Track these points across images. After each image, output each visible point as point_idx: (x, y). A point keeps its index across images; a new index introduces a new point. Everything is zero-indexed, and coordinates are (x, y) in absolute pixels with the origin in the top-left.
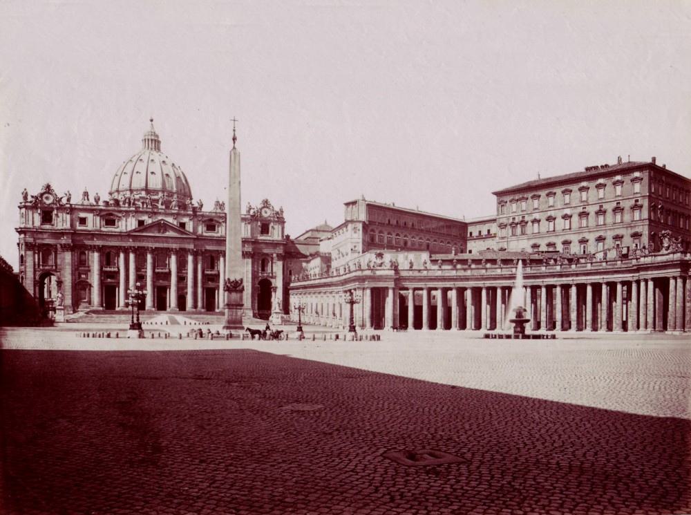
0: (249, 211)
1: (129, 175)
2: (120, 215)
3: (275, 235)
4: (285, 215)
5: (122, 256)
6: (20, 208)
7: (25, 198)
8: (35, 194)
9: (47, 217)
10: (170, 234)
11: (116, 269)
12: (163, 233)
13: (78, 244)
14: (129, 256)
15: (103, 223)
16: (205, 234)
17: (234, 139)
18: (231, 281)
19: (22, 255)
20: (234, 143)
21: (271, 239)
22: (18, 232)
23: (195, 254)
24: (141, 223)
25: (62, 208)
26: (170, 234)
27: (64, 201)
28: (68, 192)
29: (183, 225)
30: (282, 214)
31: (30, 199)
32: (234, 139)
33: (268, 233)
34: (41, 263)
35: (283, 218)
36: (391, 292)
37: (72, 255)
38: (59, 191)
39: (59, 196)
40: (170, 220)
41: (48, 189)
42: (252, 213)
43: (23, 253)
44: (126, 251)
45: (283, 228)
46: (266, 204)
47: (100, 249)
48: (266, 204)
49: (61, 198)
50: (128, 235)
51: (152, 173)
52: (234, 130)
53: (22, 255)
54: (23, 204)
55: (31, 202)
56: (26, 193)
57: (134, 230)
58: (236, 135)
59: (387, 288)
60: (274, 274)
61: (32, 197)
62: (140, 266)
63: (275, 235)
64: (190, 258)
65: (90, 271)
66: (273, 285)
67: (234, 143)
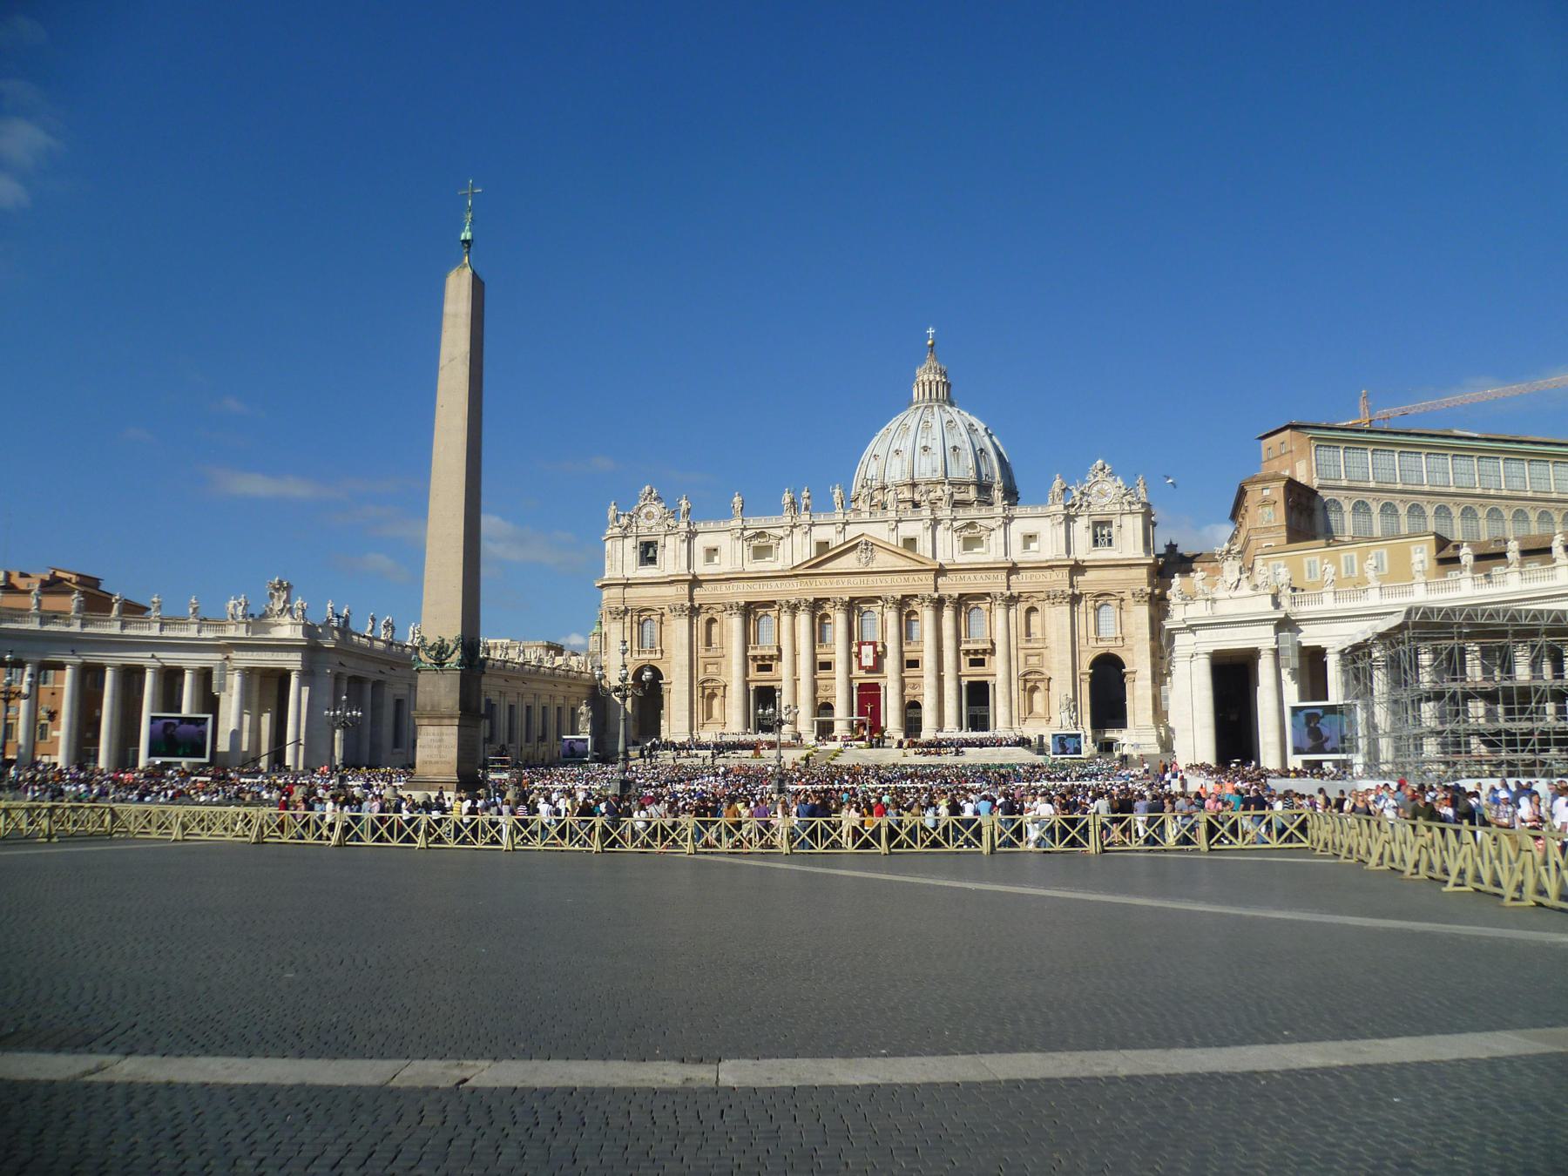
1: (881, 461)
2: (780, 532)
10: (883, 561)
11: (775, 652)
12: (867, 564)
15: (748, 553)
24: (823, 546)
29: (910, 543)
40: (879, 532)
44: (794, 609)
47: (749, 611)
51: (925, 449)
59: (1252, 656)
62: (818, 634)
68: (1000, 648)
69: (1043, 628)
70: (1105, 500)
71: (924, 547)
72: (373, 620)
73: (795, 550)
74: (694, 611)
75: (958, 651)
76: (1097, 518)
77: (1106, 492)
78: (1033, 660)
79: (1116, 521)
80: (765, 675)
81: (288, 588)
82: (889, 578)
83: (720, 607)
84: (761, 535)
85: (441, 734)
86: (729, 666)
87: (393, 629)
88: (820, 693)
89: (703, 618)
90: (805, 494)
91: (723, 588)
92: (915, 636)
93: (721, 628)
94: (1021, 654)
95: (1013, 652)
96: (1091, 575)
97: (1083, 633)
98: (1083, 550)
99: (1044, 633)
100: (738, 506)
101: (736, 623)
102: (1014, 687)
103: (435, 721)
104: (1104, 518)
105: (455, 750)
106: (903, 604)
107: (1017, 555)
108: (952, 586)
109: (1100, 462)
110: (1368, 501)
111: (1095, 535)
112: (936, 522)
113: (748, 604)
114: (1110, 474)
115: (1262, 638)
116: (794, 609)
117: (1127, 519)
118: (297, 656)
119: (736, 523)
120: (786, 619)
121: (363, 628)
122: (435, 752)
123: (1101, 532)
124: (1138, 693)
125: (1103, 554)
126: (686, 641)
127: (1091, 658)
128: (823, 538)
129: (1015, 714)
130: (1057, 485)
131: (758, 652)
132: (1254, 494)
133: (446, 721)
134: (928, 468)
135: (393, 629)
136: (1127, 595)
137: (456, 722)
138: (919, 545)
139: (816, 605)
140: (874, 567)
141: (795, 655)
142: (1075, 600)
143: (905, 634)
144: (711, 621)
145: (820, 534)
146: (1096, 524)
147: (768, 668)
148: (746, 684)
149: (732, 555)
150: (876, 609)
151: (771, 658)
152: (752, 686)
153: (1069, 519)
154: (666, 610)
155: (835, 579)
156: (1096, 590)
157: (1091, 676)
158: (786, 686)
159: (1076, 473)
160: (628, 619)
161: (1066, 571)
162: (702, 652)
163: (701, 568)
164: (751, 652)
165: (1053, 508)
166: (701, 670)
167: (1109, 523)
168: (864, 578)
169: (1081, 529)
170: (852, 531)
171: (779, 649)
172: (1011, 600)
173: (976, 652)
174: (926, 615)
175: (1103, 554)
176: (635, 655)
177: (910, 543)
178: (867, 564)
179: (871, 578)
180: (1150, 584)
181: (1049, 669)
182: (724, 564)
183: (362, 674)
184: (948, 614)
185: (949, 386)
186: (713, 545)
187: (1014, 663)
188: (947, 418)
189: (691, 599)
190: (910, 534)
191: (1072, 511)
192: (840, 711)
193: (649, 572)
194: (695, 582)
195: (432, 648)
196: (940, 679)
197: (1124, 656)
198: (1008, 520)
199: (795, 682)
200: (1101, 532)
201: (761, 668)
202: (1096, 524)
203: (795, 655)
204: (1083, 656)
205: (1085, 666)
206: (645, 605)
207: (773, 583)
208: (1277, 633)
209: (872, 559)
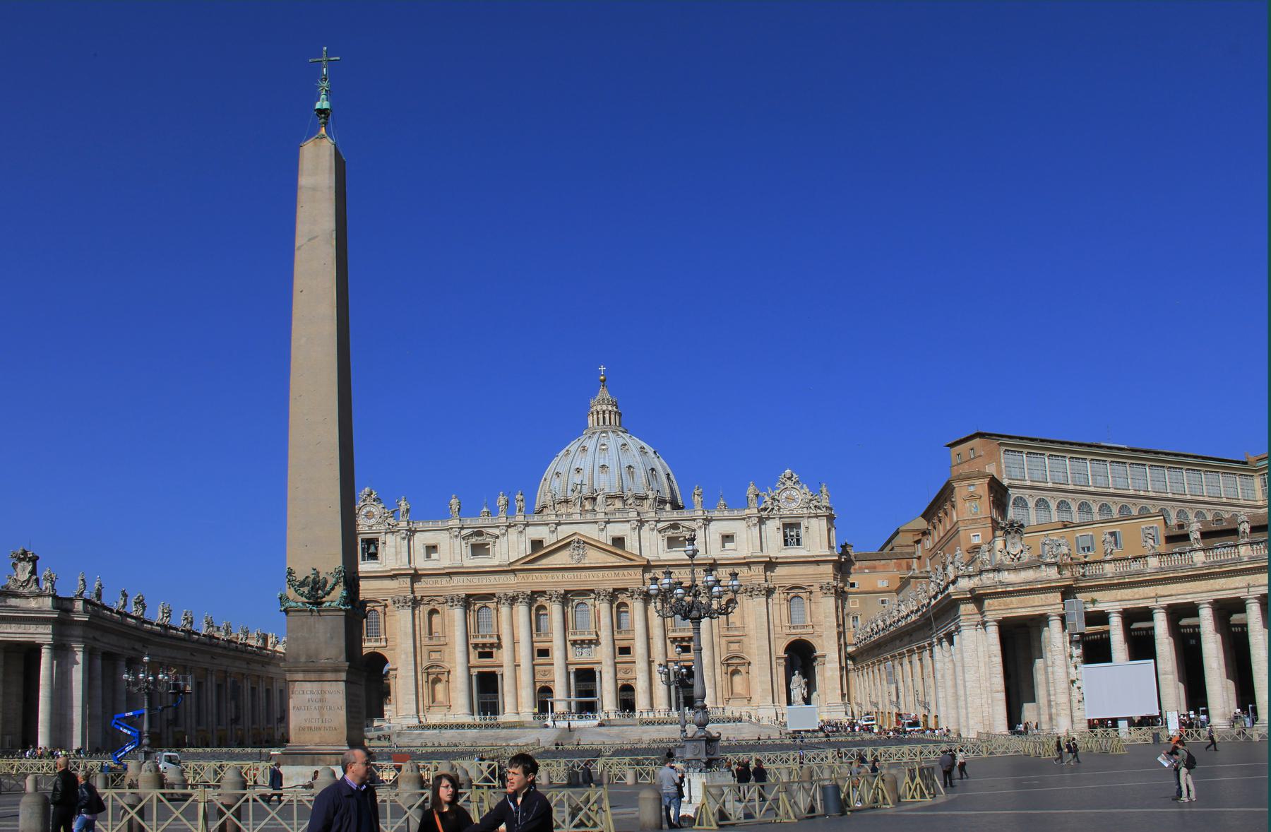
5: (504, 610)
10: (594, 558)
11: (495, 640)
12: (579, 560)
23: (647, 597)
29: (619, 542)
36: (1055, 625)
40: (590, 532)
44: (513, 600)
47: (468, 602)
59: (1040, 621)
62: (536, 626)
66: (818, 653)
69: (743, 617)
70: (794, 505)
71: (631, 545)
72: (125, 595)
73: (510, 547)
74: (416, 603)
76: (788, 521)
77: (794, 497)
78: (734, 647)
79: (804, 523)
80: (487, 661)
81: (34, 560)
82: (601, 573)
83: (442, 599)
85: (323, 692)
86: (452, 653)
87: (144, 608)
88: (538, 677)
89: (424, 610)
90: (519, 497)
91: (444, 582)
92: (624, 627)
93: (443, 619)
94: (723, 641)
95: (716, 639)
96: (779, 571)
97: (777, 622)
98: (774, 546)
99: (743, 622)
100: (455, 507)
101: (458, 612)
102: (718, 671)
103: (313, 676)
104: (793, 521)
105: (343, 712)
106: (613, 595)
109: (788, 471)
110: (1048, 499)
111: (785, 536)
112: (641, 523)
113: (468, 596)
114: (797, 482)
115: (1050, 604)
116: (513, 600)
117: (814, 521)
118: (48, 629)
119: (455, 522)
120: (504, 610)
121: (113, 601)
122: (316, 715)
123: (791, 533)
124: (828, 674)
125: (793, 552)
126: (411, 630)
127: (785, 644)
128: (537, 537)
129: (719, 694)
130: (751, 490)
131: (480, 640)
132: (961, 490)
133: (329, 676)
134: (607, 483)
135: (144, 608)
136: (816, 589)
137: (343, 676)
138: (627, 543)
139: (533, 597)
140: (586, 562)
141: (514, 642)
142: (769, 592)
143: (617, 626)
144: (433, 612)
146: (786, 526)
147: (490, 655)
149: (453, 552)
150: (589, 601)
151: (492, 645)
152: (474, 672)
153: (762, 521)
154: (390, 602)
155: (550, 574)
156: (788, 583)
157: (786, 659)
158: (507, 672)
159: (768, 480)
161: (762, 567)
162: (426, 641)
164: (472, 641)
165: (747, 511)
166: (425, 656)
167: (798, 525)
168: (577, 573)
169: (773, 527)
171: (499, 638)
174: (637, 606)
175: (793, 552)
177: (619, 542)
178: (579, 560)
179: (584, 573)
180: (835, 579)
181: (748, 654)
182: (442, 560)
183: (115, 650)
185: (620, 415)
187: (717, 649)
189: (413, 592)
190: (618, 534)
191: (764, 514)
192: (559, 691)
194: (416, 576)
195: (302, 584)
198: (708, 521)
200: (791, 533)
201: (482, 655)
203: (514, 642)
204: (779, 642)
205: (781, 653)
207: (492, 577)
208: (1063, 600)
209: (584, 556)
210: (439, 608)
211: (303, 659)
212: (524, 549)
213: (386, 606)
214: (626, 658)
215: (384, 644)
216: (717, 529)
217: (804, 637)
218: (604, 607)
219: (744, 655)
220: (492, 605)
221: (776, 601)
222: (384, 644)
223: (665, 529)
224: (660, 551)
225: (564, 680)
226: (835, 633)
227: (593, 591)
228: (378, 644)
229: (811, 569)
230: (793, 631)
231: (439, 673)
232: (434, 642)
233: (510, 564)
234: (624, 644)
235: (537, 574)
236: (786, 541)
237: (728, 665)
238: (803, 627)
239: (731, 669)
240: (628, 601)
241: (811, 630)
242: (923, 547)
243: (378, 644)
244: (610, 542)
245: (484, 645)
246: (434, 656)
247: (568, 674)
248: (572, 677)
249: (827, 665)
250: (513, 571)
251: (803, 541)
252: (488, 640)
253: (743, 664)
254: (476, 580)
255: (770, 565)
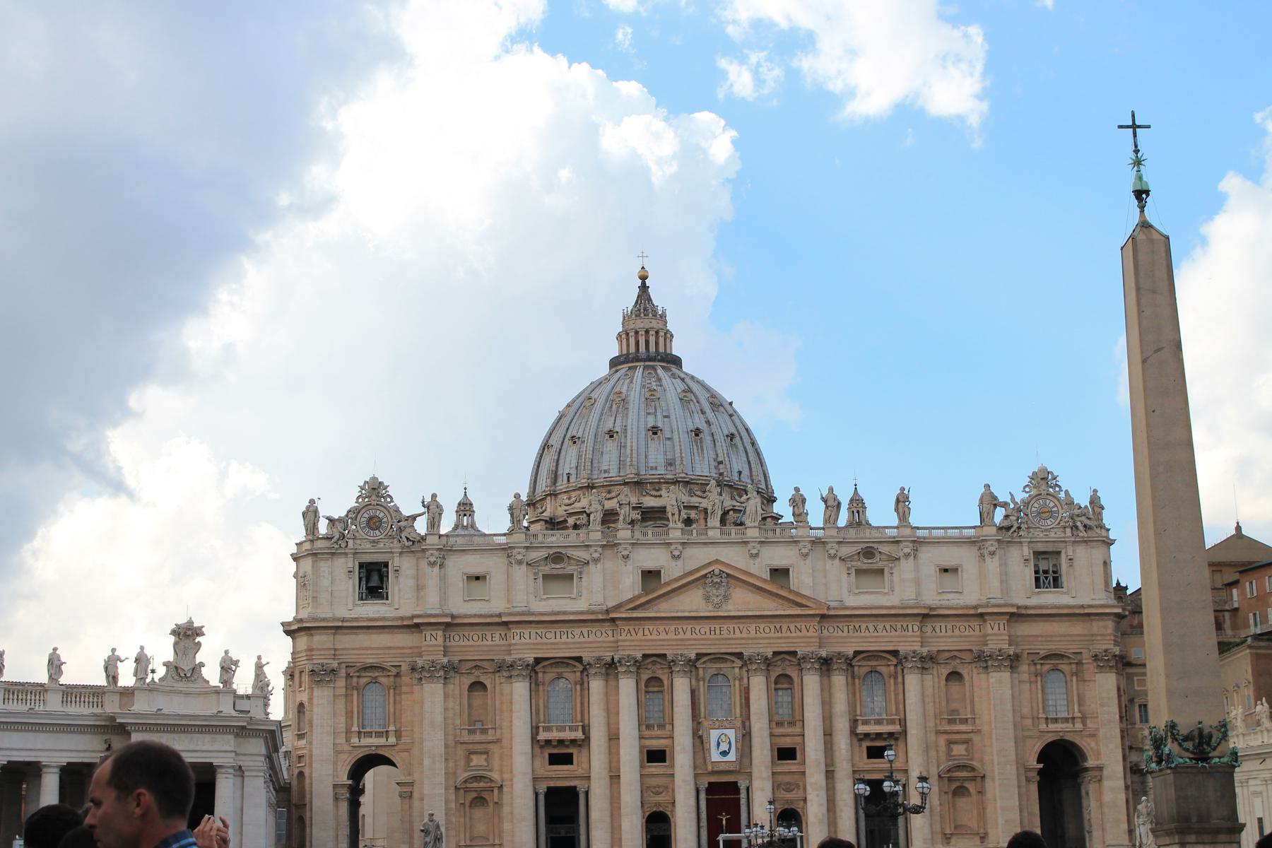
0: (985, 516)
3: (1080, 589)
4: (1107, 520)
5: (596, 685)
6: (296, 558)
7: (311, 527)
8: (339, 512)
9: (374, 580)
10: (742, 601)
11: (579, 735)
12: (718, 606)
13: (467, 659)
14: (617, 687)
16: (851, 601)
17: (1141, 194)
18: (1183, 730)
19: (301, 705)
20: (1142, 208)
21: (1071, 602)
22: (288, 633)
23: (826, 665)
24: (650, 575)
25: (415, 545)
26: (742, 601)
27: (421, 526)
28: (434, 496)
30: (1099, 516)
31: (323, 528)
32: (1141, 194)
33: (1056, 583)
34: (355, 728)
35: (1102, 527)
37: (446, 696)
38: (407, 502)
39: (406, 512)
40: (734, 557)
41: (375, 490)
42: (999, 514)
43: (304, 697)
44: (610, 668)
45: (1106, 564)
46: (1043, 480)
48: (1043, 480)
49: (414, 518)
50: (608, 619)
51: (655, 431)
52: (1138, 162)
53: (301, 705)
54: (307, 546)
55: (327, 538)
56: (316, 512)
57: (631, 601)
58: (1151, 178)
60: (1090, 724)
61: (331, 520)
63: (1080, 589)
64: (811, 682)
65: (498, 741)
66: (1090, 763)
67: (1142, 208)
68: (914, 733)
75: (853, 732)
78: (959, 750)
84: (557, 558)
91: (494, 639)
94: (942, 741)
98: (1023, 592)
101: (520, 689)
103: (1206, 838)
104: (1050, 548)
107: (931, 596)
108: (846, 641)
111: (1037, 572)
116: (610, 668)
117: (1081, 553)
120: (596, 685)
124: (1107, 797)
125: (1050, 598)
127: (1038, 746)
128: (650, 565)
131: (554, 735)
133: (1222, 837)
136: (1086, 658)
140: (730, 609)
141: (613, 737)
144: (477, 686)
145: (652, 558)
146: (1038, 554)
147: (567, 759)
148: (535, 780)
151: (573, 742)
156: (1043, 649)
157: (1040, 772)
160: (341, 683)
163: (460, 605)
164: (543, 736)
166: (462, 762)
167: (1059, 553)
168: (716, 625)
170: (697, 557)
172: (927, 662)
173: (879, 736)
174: (811, 682)
175: (1050, 598)
176: (355, 740)
177: (780, 574)
179: (727, 626)
181: (981, 761)
184: (839, 680)
186: (477, 570)
188: (680, 386)
190: (779, 562)
193: (373, 610)
194: (451, 625)
196: (830, 774)
197: (1085, 744)
199: (615, 778)
201: (555, 760)
202: (1038, 554)
205: (1033, 763)
206: (370, 660)
209: (726, 597)
210: (487, 681)
211: (1194, 819)
212: (629, 585)
213: (398, 675)
214: (788, 766)
215: (392, 740)
216: (931, 558)
217: (1068, 737)
218: (758, 685)
219: (975, 763)
220: (572, 675)
221: (1025, 677)
222: (392, 740)
223: (850, 558)
224: (845, 591)
225: (692, 801)
226: (1118, 731)
227: (739, 655)
228: (382, 741)
229: (1078, 628)
230: (1052, 727)
231: (484, 789)
232: (478, 737)
233: (607, 611)
234: (787, 742)
235: (651, 626)
236: (1037, 579)
237: (950, 779)
238: (1066, 720)
239: (954, 785)
240: (793, 673)
241: (1079, 726)
242: (1242, 594)
243: (382, 741)
244: (767, 576)
245: (561, 742)
246: (477, 760)
247: (698, 791)
248: (703, 796)
249: (1106, 783)
250: (613, 620)
251: (1064, 579)
252: (568, 735)
253: (974, 779)
254: (551, 635)
255: (1017, 616)
